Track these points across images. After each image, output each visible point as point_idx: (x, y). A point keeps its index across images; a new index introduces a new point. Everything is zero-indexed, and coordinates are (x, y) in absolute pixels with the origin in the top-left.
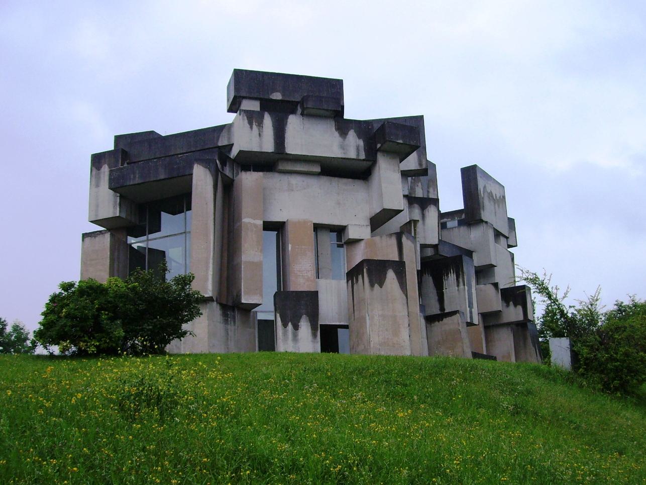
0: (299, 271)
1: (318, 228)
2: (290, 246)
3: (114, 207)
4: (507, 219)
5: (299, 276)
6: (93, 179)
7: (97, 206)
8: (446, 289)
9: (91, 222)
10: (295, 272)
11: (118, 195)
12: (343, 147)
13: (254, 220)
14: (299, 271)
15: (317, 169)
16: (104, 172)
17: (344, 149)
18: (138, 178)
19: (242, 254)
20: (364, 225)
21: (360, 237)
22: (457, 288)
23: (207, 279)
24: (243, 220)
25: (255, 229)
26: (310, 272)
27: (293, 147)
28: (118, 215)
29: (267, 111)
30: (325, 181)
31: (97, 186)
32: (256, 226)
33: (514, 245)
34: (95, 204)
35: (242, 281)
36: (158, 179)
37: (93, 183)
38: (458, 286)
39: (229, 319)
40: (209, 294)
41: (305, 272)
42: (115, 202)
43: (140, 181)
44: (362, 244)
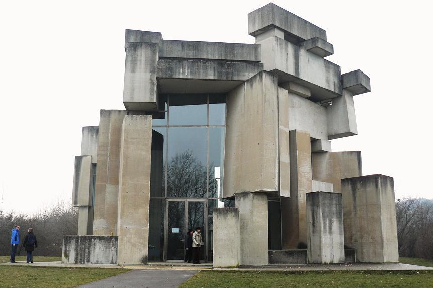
2: (297, 151)
3: (152, 94)
6: (129, 63)
12: (328, 81)
16: (141, 61)
17: (328, 83)
27: (304, 76)
29: (290, 42)
30: (308, 101)
31: (133, 71)
36: (207, 78)
37: (129, 67)
42: (152, 90)
43: (189, 77)
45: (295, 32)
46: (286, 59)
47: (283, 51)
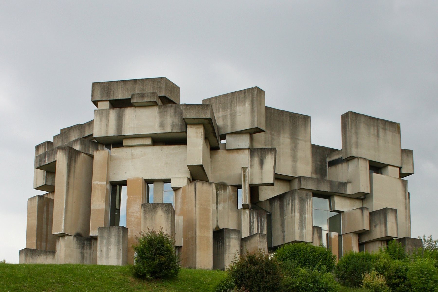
0: (132, 213)
1: (148, 182)
3: (44, 180)
4: (399, 151)
5: (132, 215)
7: (37, 179)
8: (286, 216)
9: (35, 189)
10: (130, 213)
11: (45, 171)
12: (162, 125)
13: (100, 182)
14: (132, 213)
15: (149, 141)
17: (163, 127)
18: (47, 160)
19: (91, 204)
20: (182, 177)
21: (179, 185)
22: (291, 215)
23: (61, 222)
24: (93, 183)
25: (101, 188)
26: (138, 213)
28: (45, 184)
30: (157, 148)
32: (101, 186)
33: (409, 172)
34: (36, 179)
35: (91, 222)
38: (292, 213)
39: (85, 246)
40: (61, 231)
41: (135, 213)
42: (44, 175)
44: (181, 190)
45: (120, 96)
46: (107, 125)
47: (104, 119)
